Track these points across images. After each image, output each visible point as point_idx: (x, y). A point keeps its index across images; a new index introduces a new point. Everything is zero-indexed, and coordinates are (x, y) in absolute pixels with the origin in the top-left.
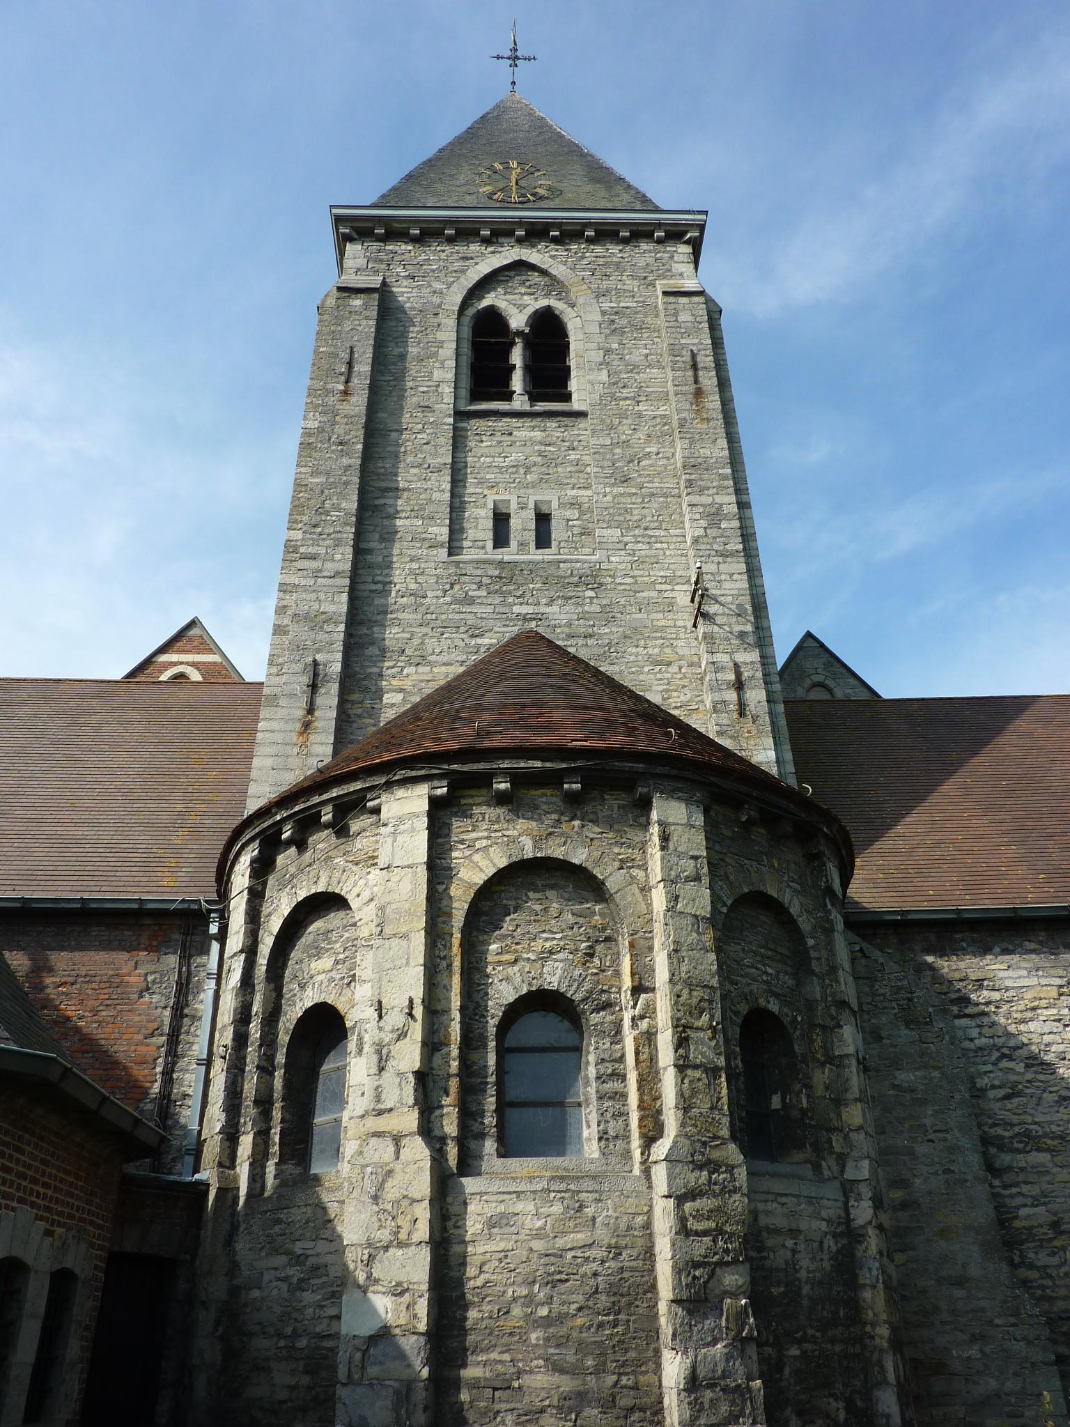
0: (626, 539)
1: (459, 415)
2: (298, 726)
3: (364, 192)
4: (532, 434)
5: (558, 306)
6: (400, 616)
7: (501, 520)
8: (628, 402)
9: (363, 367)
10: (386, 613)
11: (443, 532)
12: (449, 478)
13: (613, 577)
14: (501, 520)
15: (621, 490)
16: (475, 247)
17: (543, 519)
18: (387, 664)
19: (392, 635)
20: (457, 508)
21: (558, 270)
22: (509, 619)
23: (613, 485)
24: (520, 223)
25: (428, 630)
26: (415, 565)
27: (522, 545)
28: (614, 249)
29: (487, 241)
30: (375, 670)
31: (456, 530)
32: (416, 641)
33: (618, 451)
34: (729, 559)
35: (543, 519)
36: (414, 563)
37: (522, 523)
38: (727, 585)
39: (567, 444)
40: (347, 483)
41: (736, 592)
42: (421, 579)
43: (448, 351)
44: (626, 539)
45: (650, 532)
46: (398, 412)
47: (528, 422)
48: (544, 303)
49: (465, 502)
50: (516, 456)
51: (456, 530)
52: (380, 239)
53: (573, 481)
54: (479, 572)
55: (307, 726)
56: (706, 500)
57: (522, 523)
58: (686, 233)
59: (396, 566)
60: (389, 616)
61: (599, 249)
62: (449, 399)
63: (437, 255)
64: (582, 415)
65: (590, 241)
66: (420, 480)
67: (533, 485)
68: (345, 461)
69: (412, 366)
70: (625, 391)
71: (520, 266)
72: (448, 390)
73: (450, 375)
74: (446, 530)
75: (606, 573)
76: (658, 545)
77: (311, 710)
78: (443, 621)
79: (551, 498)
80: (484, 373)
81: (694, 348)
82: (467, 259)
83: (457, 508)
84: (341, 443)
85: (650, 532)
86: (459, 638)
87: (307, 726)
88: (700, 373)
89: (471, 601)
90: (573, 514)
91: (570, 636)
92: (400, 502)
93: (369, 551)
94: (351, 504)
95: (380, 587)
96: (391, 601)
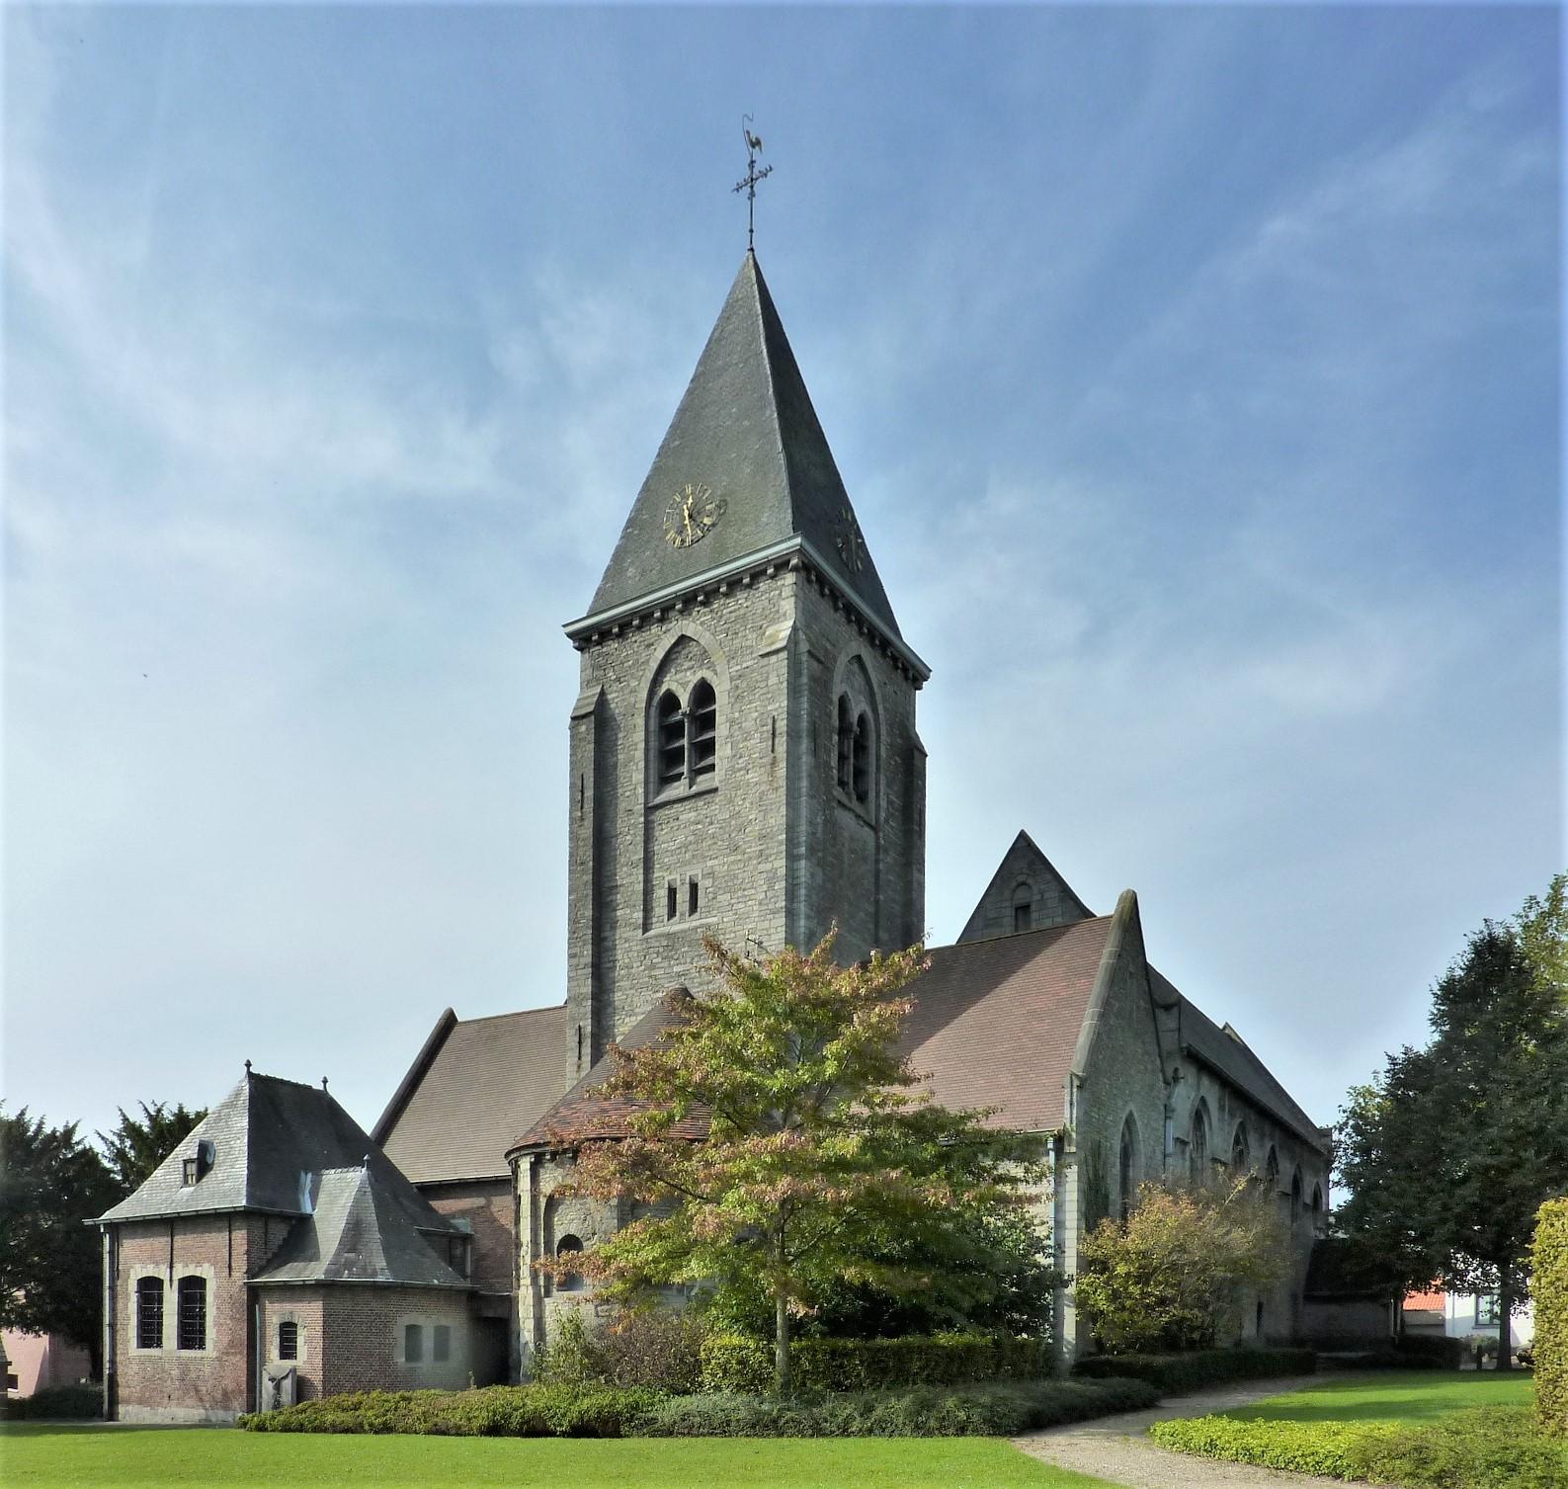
0: (733, 901)
1: (649, 810)
2: (576, 1068)
3: (578, 607)
4: (690, 815)
5: (708, 675)
6: (622, 984)
7: (672, 892)
8: (742, 773)
9: (589, 793)
10: (614, 983)
11: (639, 915)
12: (642, 871)
13: (724, 934)
14: (672, 892)
15: (732, 858)
16: (655, 629)
17: (694, 887)
18: (617, 1018)
19: (618, 997)
20: (648, 893)
21: (705, 639)
22: (670, 977)
23: (728, 855)
24: (677, 597)
25: (633, 991)
26: (627, 945)
27: (682, 915)
28: (741, 596)
29: (662, 620)
30: (612, 1023)
31: (647, 910)
32: (629, 1000)
33: (733, 822)
34: (777, 916)
35: (694, 887)
36: (627, 943)
37: (683, 897)
38: (773, 937)
39: (708, 820)
40: (587, 895)
41: (777, 942)
42: (630, 955)
43: (640, 754)
44: (733, 901)
45: (746, 893)
46: (614, 822)
47: (688, 805)
48: (699, 676)
49: (653, 885)
50: (682, 838)
51: (647, 910)
52: (599, 643)
53: (711, 853)
54: (657, 944)
55: (579, 1067)
56: (769, 866)
57: (683, 897)
58: (789, 561)
59: (618, 947)
60: (617, 985)
61: (731, 601)
62: (641, 800)
63: (635, 638)
64: (716, 790)
65: (727, 595)
66: (628, 878)
67: (689, 863)
68: (585, 878)
69: (621, 772)
70: (740, 761)
71: (683, 640)
72: (641, 790)
73: (642, 777)
74: (641, 914)
75: (720, 932)
76: (750, 903)
77: (580, 1058)
78: (641, 984)
79: (695, 871)
80: (666, 764)
81: (775, 713)
82: (649, 646)
83: (648, 893)
84: (582, 864)
85: (746, 893)
86: (648, 995)
87: (579, 1067)
88: (777, 740)
89: (653, 966)
90: (708, 882)
91: (701, 984)
92: (619, 896)
93: (605, 939)
94: (589, 913)
95: (611, 964)
96: (617, 974)
